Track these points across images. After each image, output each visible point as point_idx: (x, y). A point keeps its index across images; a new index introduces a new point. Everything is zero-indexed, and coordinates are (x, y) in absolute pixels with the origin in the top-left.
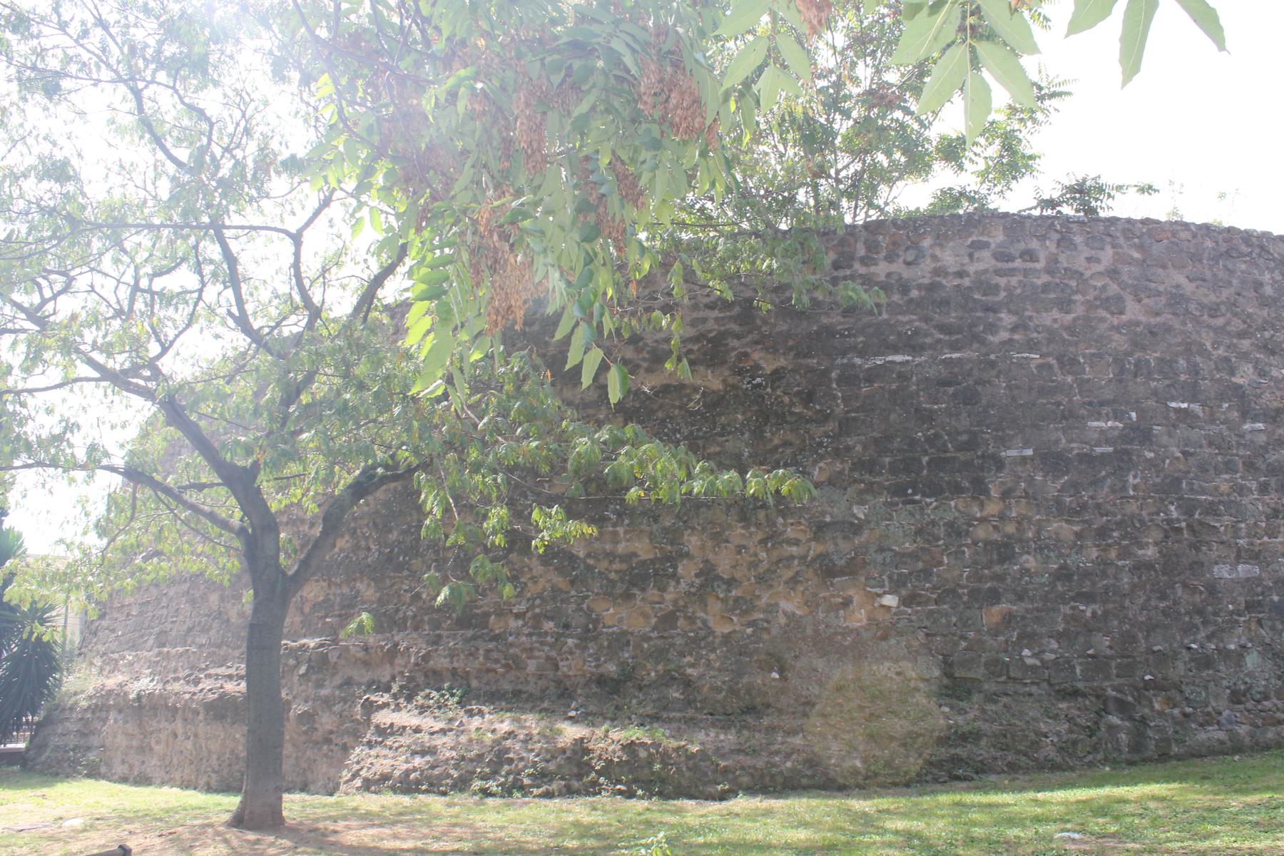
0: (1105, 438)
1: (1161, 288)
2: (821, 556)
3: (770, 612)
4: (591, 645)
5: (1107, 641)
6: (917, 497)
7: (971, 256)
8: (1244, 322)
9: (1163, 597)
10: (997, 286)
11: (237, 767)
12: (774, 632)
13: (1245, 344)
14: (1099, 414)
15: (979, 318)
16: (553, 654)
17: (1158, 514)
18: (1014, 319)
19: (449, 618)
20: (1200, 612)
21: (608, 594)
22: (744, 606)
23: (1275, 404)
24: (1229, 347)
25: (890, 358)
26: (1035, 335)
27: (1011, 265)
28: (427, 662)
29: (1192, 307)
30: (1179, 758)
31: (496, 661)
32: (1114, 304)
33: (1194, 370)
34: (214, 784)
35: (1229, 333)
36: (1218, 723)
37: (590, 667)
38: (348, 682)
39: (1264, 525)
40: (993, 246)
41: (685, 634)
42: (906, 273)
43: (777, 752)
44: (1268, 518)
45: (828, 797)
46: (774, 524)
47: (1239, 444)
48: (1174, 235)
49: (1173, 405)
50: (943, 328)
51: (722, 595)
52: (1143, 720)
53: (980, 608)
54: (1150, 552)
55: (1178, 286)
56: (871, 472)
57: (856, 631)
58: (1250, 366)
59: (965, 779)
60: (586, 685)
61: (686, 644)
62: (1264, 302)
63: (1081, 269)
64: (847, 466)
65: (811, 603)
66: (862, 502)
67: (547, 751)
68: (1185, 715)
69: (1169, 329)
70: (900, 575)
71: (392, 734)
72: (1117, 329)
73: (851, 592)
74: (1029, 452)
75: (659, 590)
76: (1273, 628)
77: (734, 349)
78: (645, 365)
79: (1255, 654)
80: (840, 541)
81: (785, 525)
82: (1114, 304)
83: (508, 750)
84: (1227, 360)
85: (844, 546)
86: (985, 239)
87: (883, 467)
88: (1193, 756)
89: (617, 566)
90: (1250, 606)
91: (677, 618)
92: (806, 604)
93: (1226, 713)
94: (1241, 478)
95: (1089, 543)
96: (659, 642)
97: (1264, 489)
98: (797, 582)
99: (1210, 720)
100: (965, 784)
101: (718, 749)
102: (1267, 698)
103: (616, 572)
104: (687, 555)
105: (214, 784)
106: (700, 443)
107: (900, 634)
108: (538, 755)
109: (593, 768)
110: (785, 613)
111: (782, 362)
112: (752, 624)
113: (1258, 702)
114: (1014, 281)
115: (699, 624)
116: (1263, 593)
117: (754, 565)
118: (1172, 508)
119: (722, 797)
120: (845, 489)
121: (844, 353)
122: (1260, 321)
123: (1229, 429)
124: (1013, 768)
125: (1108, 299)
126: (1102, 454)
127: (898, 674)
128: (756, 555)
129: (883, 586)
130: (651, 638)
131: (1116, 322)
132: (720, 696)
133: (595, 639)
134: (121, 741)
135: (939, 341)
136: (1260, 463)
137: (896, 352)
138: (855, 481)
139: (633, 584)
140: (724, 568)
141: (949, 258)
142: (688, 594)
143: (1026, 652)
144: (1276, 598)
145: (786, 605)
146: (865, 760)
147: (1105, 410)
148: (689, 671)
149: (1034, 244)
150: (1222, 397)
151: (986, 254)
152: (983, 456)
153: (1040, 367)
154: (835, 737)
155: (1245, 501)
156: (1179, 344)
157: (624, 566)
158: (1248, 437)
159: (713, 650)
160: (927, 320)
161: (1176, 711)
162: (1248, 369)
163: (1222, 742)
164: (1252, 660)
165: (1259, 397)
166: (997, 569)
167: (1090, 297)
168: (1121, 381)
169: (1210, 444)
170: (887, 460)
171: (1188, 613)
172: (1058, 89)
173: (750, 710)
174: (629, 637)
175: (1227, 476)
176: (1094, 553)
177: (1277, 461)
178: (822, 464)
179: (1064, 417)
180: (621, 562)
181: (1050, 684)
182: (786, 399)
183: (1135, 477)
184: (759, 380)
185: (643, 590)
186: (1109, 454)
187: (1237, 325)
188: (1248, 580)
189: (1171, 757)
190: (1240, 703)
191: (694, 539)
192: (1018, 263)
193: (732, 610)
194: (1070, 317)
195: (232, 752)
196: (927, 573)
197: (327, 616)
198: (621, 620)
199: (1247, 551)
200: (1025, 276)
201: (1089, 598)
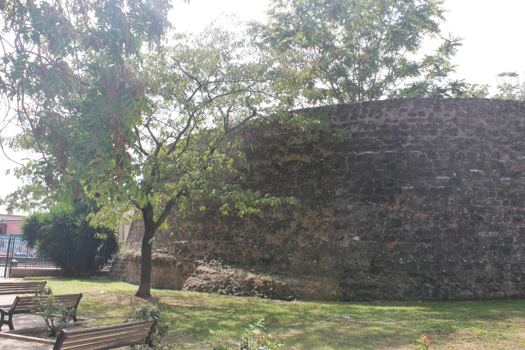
0: (442, 182)
1: (474, 125)
2: (336, 222)
5: (432, 257)
7: (400, 114)
8: (508, 138)
9: (456, 242)
10: (408, 126)
12: (318, 247)
13: (507, 147)
14: (441, 174)
15: (400, 138)
16: (250, 250)
17: (459, 212)
18: (413, 138)
20: (471, 249)
22: (309, 237)
23: (517, 170)
24: (499, 148)
25: (366, 152)
26: (420, 144)
27: (414, 118)
29: (486, 133)
30: (452, 300)
31: (234, 251)
32: (454, 132)
33: (483, 157)
34: (154, 286)
35: (501, 143)
36: (470, 289)
37: (260, 255)
39: (503, 217)
40: (409, 110)
41: (290, 246)
42: (376, 121)
43: (309, 287)
44: (505, 214)
45: (344, 304)
47: (497, 186)
48: (482, 104)
49: (472, 170)
50: (386, 142)
52: (439, 286)
53: (387, 243)
54: (454, 226)
55: (481, 124)
57: (345, 248)
58: (508, 155)
59: (368, 301)
60: (259, 261)
62: (519, 130)
63: (442, 119)
64: (348, 191)
65: (331, 238)
66: (351, 204)
67: (241, 281)
68: (457, 286)
69: (474, 141)
70: (361, 230)
71: (200, 273)
72: (453, 141)
73: (344, 235)
74: (412, 188)
76: (500, 256)
77: (315, 148)
78: (286, 153)
79: (490, 265)
82: (454, 132)
83: (230, 280)
84: (498, 153)
85: (344, 219)
86: (406, 108)
88: (458, 300)
90: (492, 247)
91: (289, 241)
93: (474, 286)
94: (496, 199)
95: (430, 221)
96: (282, 248)
97: (505, 203)
99: (466, 288)
100: (368, 302)
101: (292, 284)
102: (492, 281)
104: (294, 219)
105: (154, 286)
106: (301, 181)
107: (358, 250)
110: (322, 241)
111: (330, 153)
112: (311, 244)
113: (488, 282)
114: (415, 124)
115: (295, 243)
116: (498, 243)
118: (465, 210)
119: (290, 300)
121: (351, 151)
122: (516, 137)
123: (494, 180)
124: (385, 299)
125: (451, 130)
126: (440, 189)
127: (356, 264)
128: (315, 220)
129: (355, 233)
131: (453, 139)
132: (297, 267)
134: (132, 271)
135: (385, 146)
136: (506, 194)
137: (369, 150)
140: (304, 225)
141: (392, 115)
142: (293, 233)
143: (401, 259)
144: (503, 245)
146: (337, 292)
147: (444, 172)
148: (289, 258)
149: (425, 109)
150: (493, 167)
151: (405, 113)
152: (395, 189)
153: (421, 156)
154: (329, 283)
155: (497, 208)
156: (478, 147)
157: (274, 222)
158: (502, 183)
159: (298, 252)
160: (381, 138)
161: (453, 284)
162: (507, 157)
163: (470, 296)
164: (488, 268)
165: (510, 167)
166: (395, 229)
167: (444, 129)
168: (452, 161)
169: (485, 186)
170: (361, 189)
171: (466, 249)
172: (457, 42)
173: (305, 273)
175: (490, 198)
176: (432, 225)
177: (513, 192)
179: (427, 175)
181: (408, 271)
182: (330, 166)
183: (452, 198)
184: (322, 159)
185: (279, 230)
186: (442, 189)
187: (505, 139)
188: (492, 237)
189: (448, 300)
190: (480, 282)
191: (296, 214)
192: (417, 117)
193: (306, 239)
194: (435, 137)
195: (160, 276)
196: (370, 230)
199: (494, 227)
200: (419, 121)
201: (427, 241)
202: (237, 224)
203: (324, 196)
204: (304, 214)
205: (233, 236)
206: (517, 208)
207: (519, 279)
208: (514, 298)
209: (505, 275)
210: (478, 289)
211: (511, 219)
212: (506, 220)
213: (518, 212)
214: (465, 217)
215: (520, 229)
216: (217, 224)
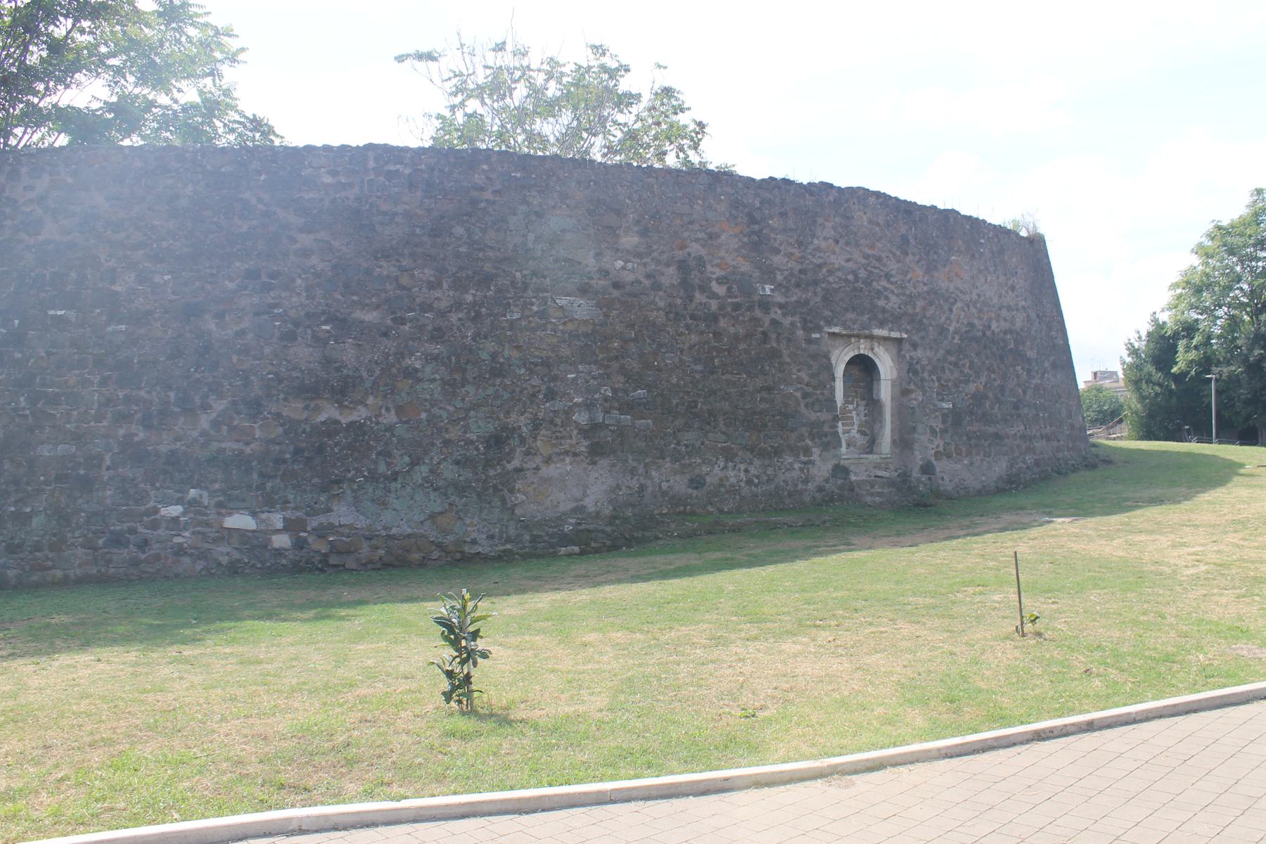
17: (10, 403)
49: (52, 312)
94: (89, 373)
97: (104, 382)
102: (39, 549)
162: (131, 277)
164: (36, 522)
175: (77, 372)
206: (127, 392)
207: (101, 542)
208: (82, 581)
209: (70, 535)
210: (9, 568)
211: (110, 415)
212: (99, 418)
213: (127, 399)
214: (20, 416)
215: (124, 436)
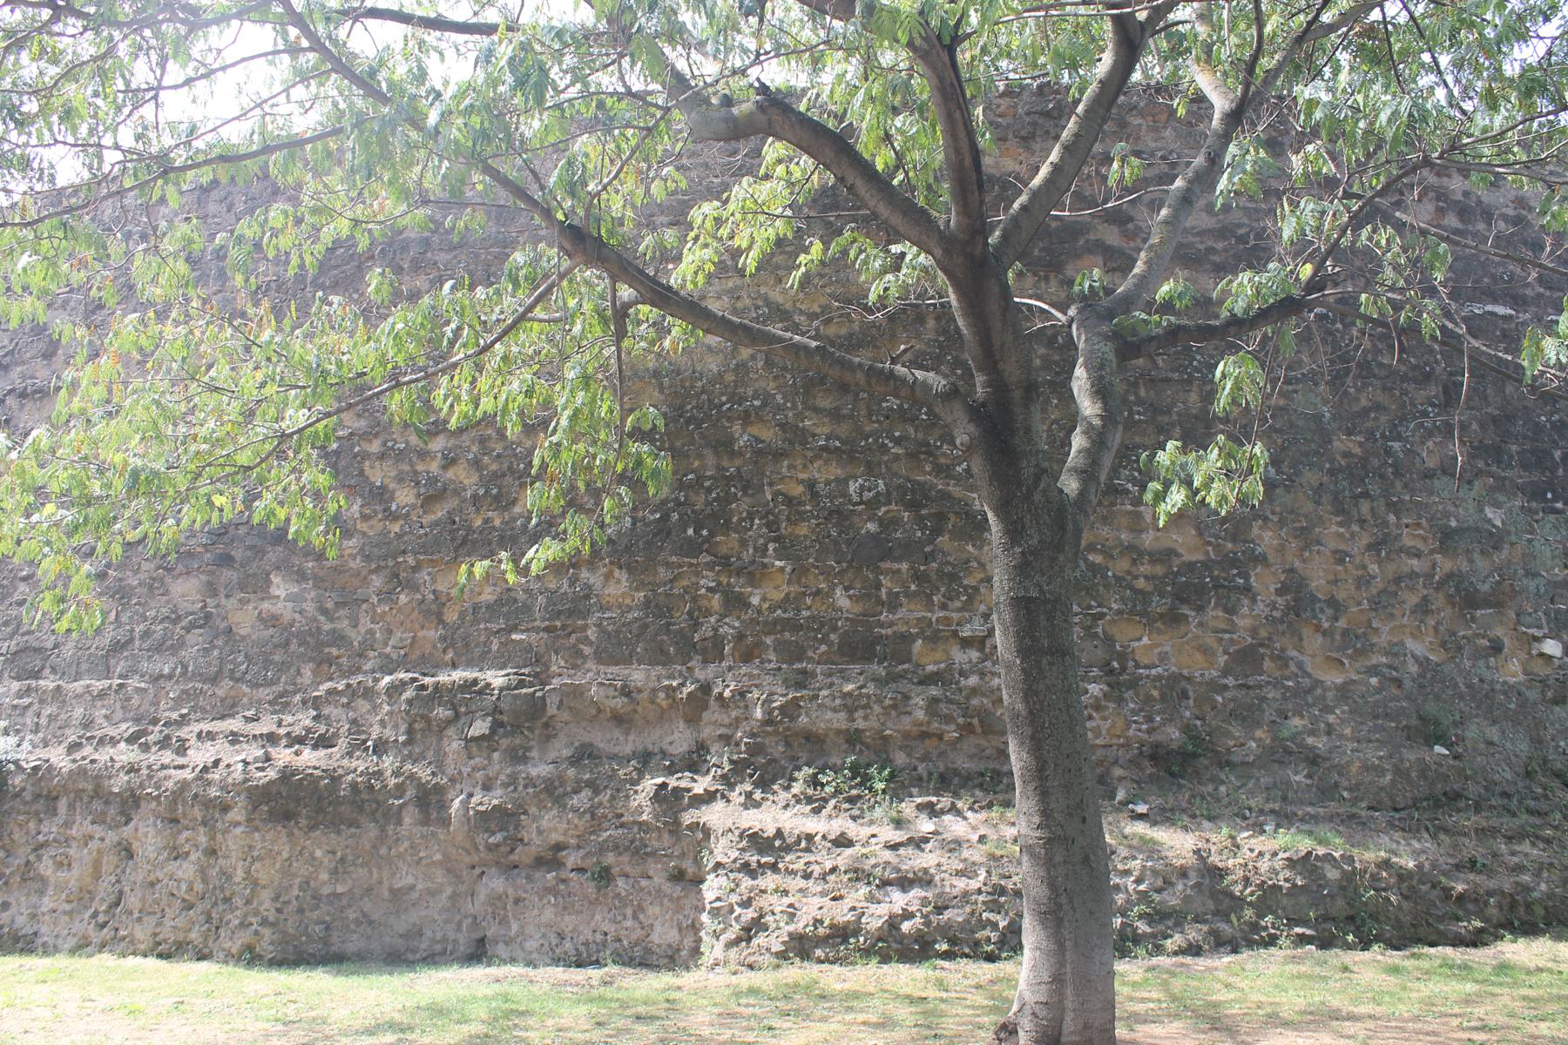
3: (1395, 655)
4: (1128, 694)
6: (1559, 505)
11: (315, 915)
12: (1408, 684)
19: (823, 641)
21: (1138, 609)
28: (793, 718)
31: (948, 719)
34: (265, 947)
38: (584, 754)
41: (1277, 684)
46: (1385, 523)
51: (1326, 625)
56: (1499, 462)
60: (1134, 763)
61: (1285, 699)
65: (1450, 645)
67: (1155, 872)
71: (788, 849)
73: (1499, 632)
75: (1226, 610)
80: (1476, 556)
81: (1398, 526)
85: (1482, 564)
87: (1511, 457)
89: (1144, 568)
92: (1443, 644)
98: (1427, 612)
103: (1146, 577)
104: (1262, 560)
105: (265, 947)
108: (1138, 881)
109: (1242, 899)
112: (1373, 670)
115: (1293, 668)
117: (1363, 581)
119: (1476, 940)
120: (1469, 482)
128: (1364, 567)
130: (1226, 687)
133: (1133, 684)
135: (1540, 295)
137: (1495, 301)
138: (1479, 473)
139: (1181, 597)
140: (1318, 582)
145: (1415, 646)
157: (1159, 570)
174: (1184, 684)
178: (1430, 444)
180: (1153, 562)
185: (1200, 609)
197: (514, 629)
198: (1163, 658)
202: (919, 577)
203: (1376, 463)
204: (1307, 537)
205: (907, 639)
216: (755, 573)
